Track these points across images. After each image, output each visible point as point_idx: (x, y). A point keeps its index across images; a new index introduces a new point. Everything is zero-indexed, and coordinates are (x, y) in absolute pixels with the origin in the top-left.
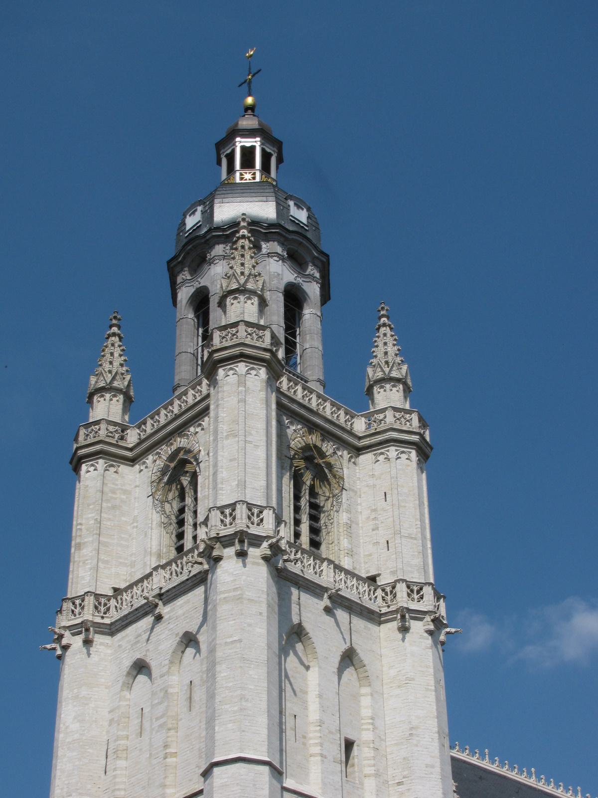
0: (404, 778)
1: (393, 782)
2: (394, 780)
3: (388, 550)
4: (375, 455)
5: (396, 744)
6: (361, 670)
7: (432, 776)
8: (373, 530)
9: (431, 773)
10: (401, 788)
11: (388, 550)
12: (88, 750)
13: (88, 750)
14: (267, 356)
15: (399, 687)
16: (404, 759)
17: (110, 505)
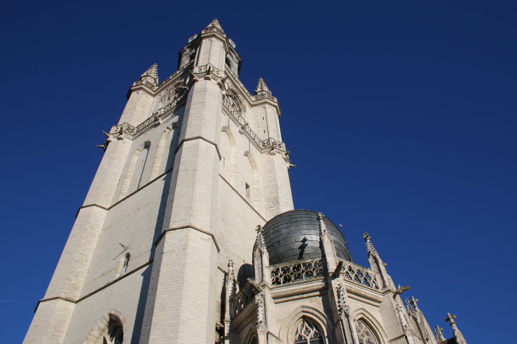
0: (274, 205)
1: (268, 207)
2: (269, 206)
3: (265, 133)
4: (259, 107)
5: (270, 193)
6: (253, 163)
7: (288, 206)
8: (258, 127)
9: (287, 205)
10: (272, 209)
11: (265, 133)
12: (112, 176)
13: (112, 176)
14: (224, 40)
15: (270, 173)
16: (274, 198)
17: (141, 105)
